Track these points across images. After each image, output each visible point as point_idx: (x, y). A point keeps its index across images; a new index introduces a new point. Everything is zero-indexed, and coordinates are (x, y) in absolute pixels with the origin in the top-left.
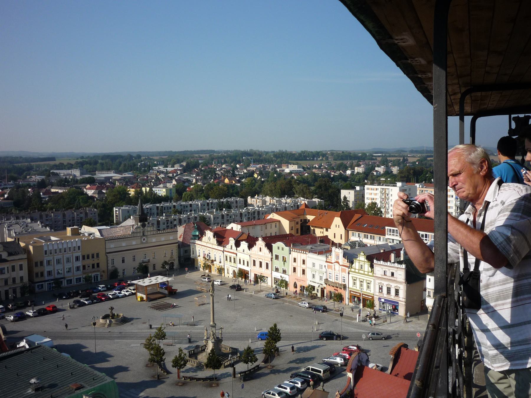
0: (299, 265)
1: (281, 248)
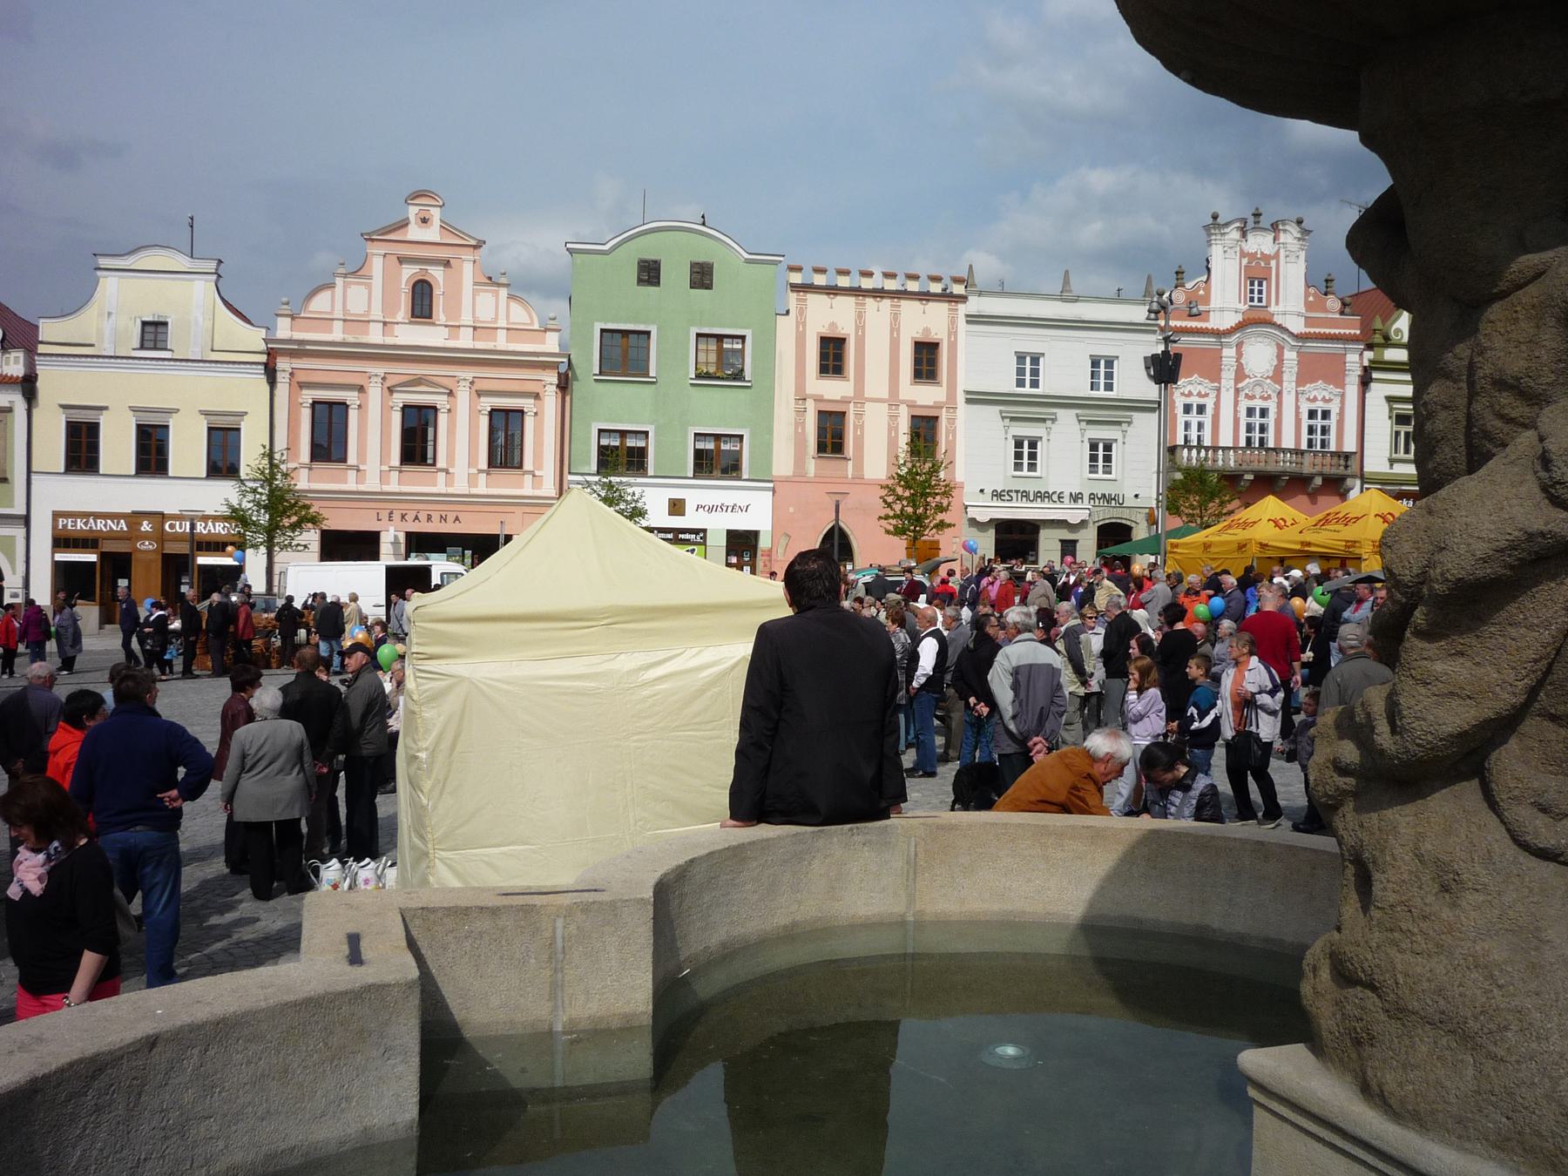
0: (877, 384)
1: (675, 274)
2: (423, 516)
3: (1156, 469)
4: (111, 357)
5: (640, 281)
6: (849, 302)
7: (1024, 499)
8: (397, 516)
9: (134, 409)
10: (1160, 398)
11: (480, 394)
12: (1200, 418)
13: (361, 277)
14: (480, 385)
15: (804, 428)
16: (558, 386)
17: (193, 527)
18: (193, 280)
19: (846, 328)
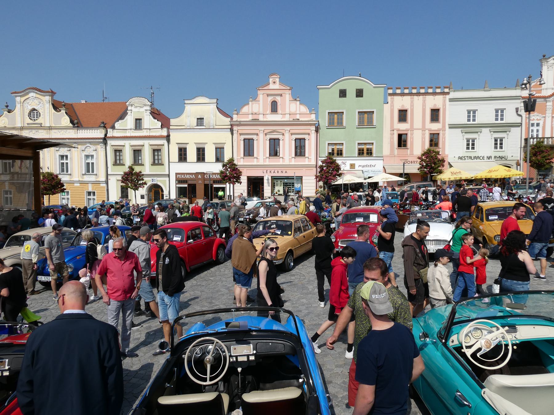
2: (276, 171)
3: (520, 146)
4: (189, 129)
5: (340, 96)
6: (408, 98)
7: (470, 159)
8: (268, 172)
9: (196, 143)
10: (522, 121)
11: (292, 134)
12: (538, 128)
13: (256, 101)
14: (292, 131)
15: (393, 140)
16: (315, 131)
17: (209, 176)
18: (210, 105)
19: (407, 106)
